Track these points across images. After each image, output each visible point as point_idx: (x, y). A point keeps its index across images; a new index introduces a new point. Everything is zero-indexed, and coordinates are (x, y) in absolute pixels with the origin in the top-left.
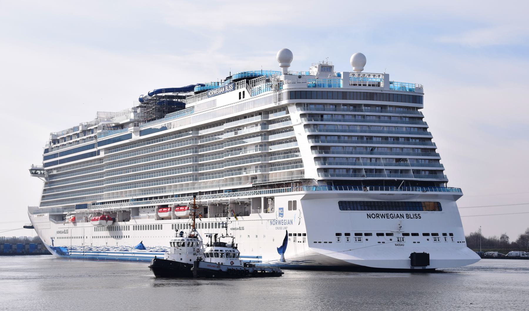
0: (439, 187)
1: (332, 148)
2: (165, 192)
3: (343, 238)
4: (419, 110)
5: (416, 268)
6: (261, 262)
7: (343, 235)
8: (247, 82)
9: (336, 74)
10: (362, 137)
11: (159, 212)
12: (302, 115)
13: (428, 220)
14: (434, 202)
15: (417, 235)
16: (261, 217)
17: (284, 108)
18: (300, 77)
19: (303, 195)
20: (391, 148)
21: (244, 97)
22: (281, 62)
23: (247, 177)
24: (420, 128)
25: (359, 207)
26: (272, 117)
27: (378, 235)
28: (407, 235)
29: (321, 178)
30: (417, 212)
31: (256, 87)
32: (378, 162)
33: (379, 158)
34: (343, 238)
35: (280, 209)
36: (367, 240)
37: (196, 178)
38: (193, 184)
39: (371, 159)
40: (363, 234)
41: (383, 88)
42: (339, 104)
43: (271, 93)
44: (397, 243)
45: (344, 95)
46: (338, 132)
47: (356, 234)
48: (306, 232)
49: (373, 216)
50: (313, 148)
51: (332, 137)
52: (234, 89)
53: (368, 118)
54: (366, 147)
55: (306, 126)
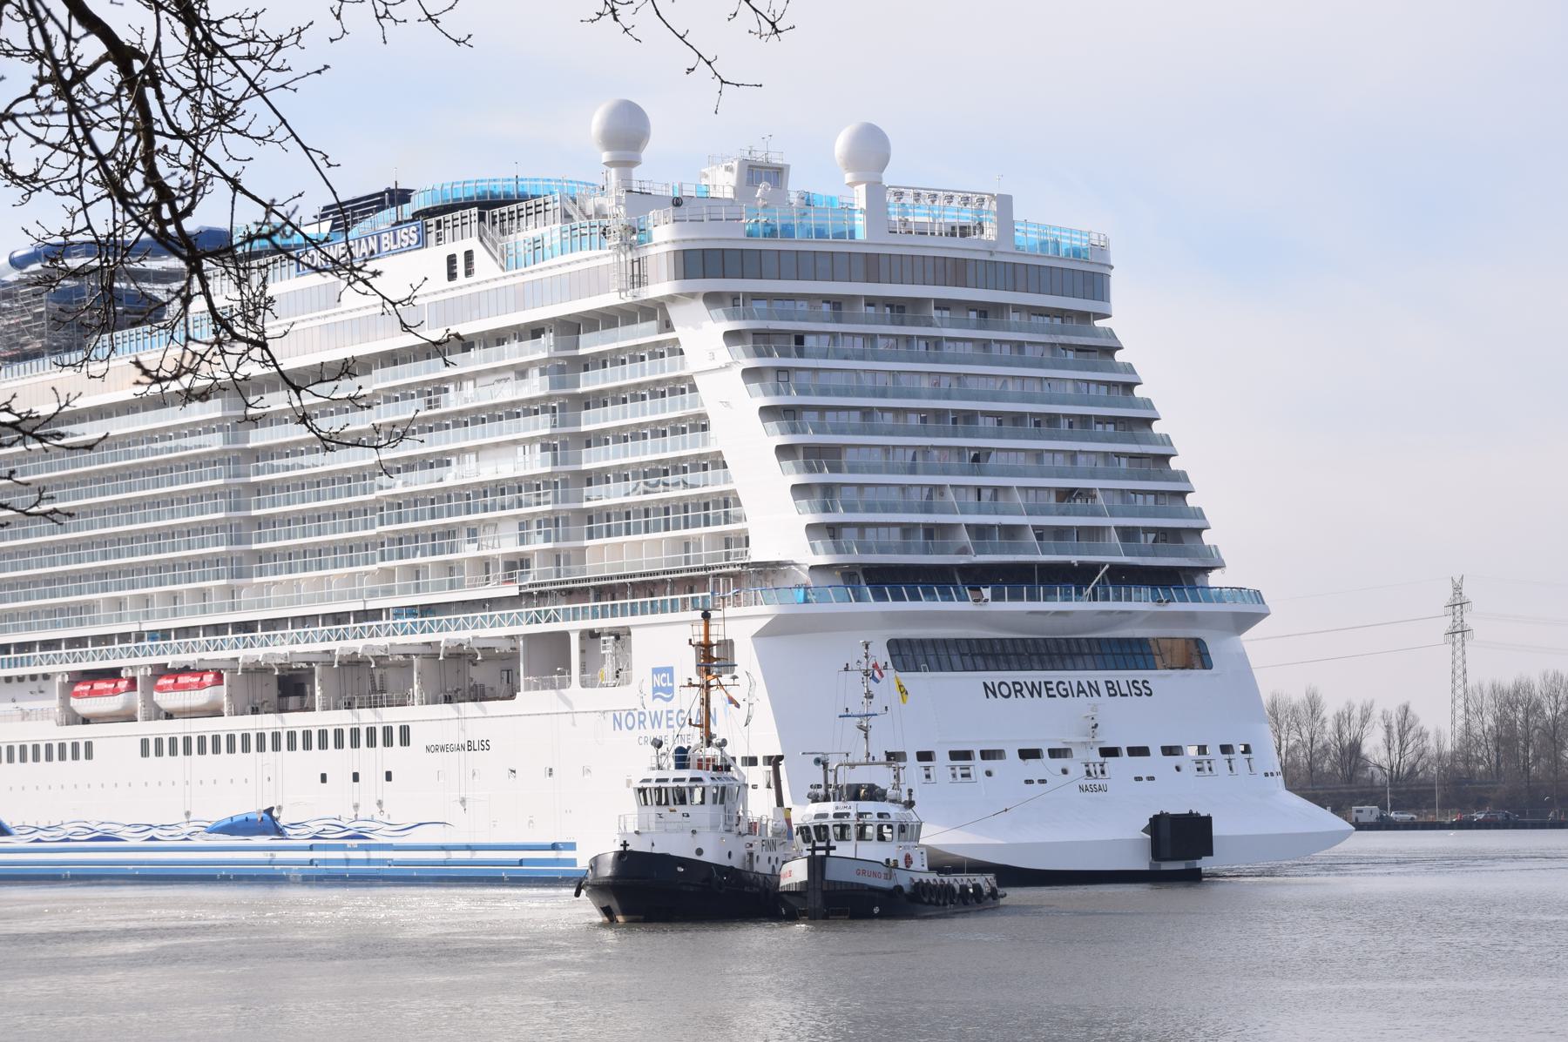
0: (1193, 587)
1: (849, 450)
2: (93, 622)
4: (1098, 323)
6: (573, 862)
7: (912, 756)
8: (482, 218)
9: (794, 198)
10: (940, 414)
11: (77, 695)
12: (732, 337)
14: (1187, 640)
16: (567, 702)
17: (652, 311)
18: (677, 202)
19: (761, 623)
20: (1039, 454)
21: (468, 273)
22: (608, 149)
23: (486, 565)
24: (1115, 384)
25: (956, 660)
26: (590, 345)
27: (1026, 754)
29: (823, 559)
31: (521, 236)
32: (1001, 500)
33: (1007, 489)
35: (656, 671)
37: (239, 567)
38: (232, 592)
39: (979, 490)
41: (996, 243)
42: (853, 299)
43: (605, 257)
45: (872, 265)
46: (861, 393)
47: (954, 755)
48: (776, 751)
50: (783, 451)
51: (843, 415)
52: (423, 242)
53: (948, 348)
54: (960, 449)
55: (750, 374)
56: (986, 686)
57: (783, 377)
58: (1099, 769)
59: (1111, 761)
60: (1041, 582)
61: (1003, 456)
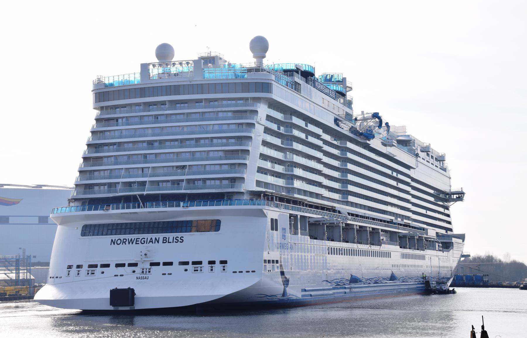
3: (74, 270)
5: (121, 308)
7: (75, 267)
13: (195, 245)
14: (212, 220)
15: (171, 264)
24: (241, 124)
27: (118, 265)
28: (158, 264)
30: (179, 235)
34: (74, 270)
39: (143, 169)
40: (99, 266)
44: (139, 276)
47: (90, 266)
49: (119, 242)
56: (112, 240)
57: (101, 134)
58: (148, 270)
59: (154, 267)
60: (189, 200)
61: (163, 155)
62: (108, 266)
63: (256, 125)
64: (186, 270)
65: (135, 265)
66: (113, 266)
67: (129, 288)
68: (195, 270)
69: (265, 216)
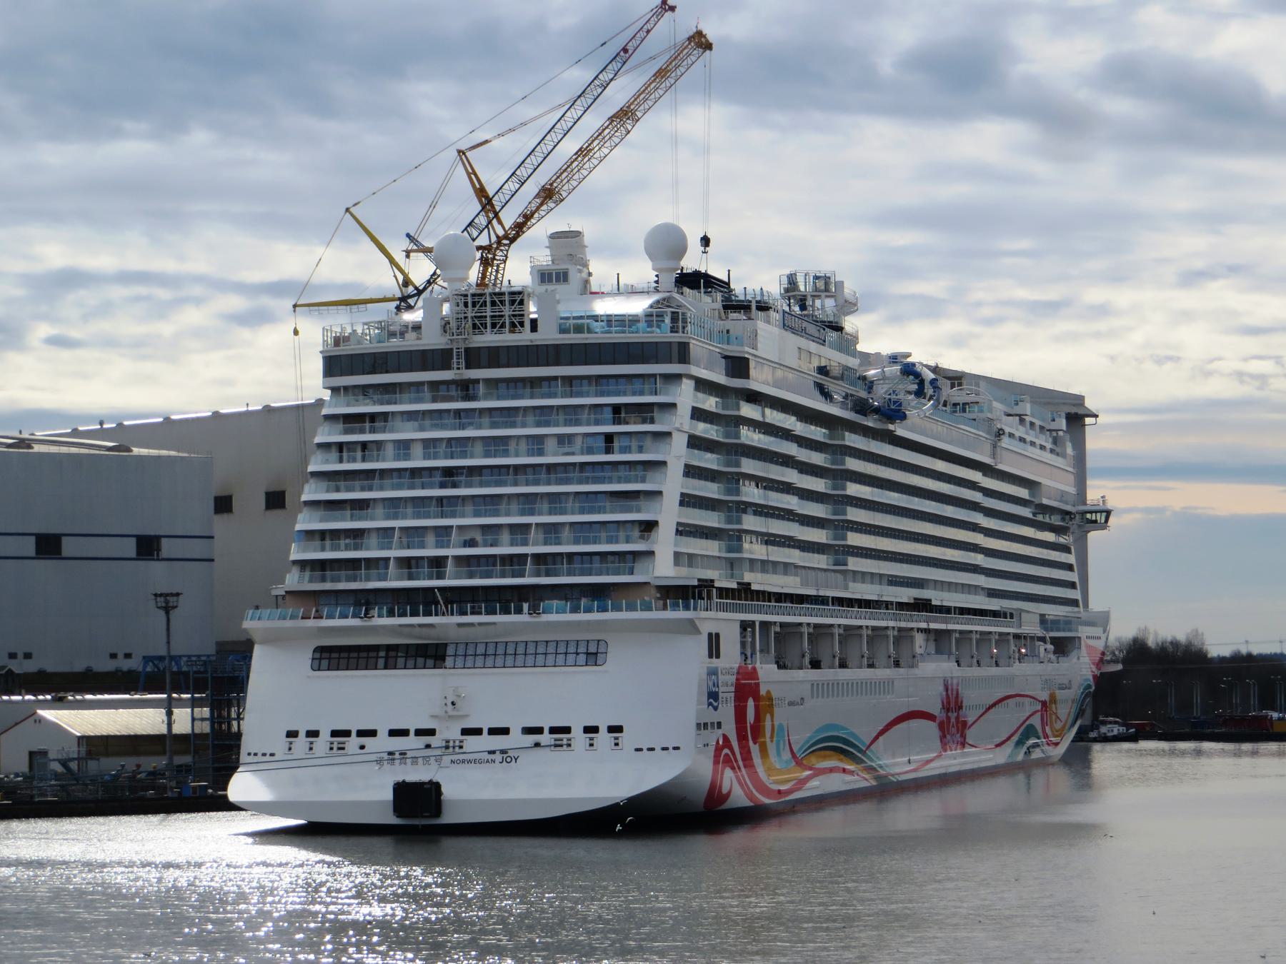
3: (302, 741)
7: (302, 734)
15: (505, 731)
27: (393, 733)
28: (478, 732)
34: (302, 741)
36: (362, 747)
40: (354, 734)
47: (335, 733)
59: (471, 741)
62: (372, 733)
63: (675, 435)
64: (537, 745)
65: (431, 732)
66: (382, 733)
67: (431, 782)
68: (556, 746)
69: (699, 632)
